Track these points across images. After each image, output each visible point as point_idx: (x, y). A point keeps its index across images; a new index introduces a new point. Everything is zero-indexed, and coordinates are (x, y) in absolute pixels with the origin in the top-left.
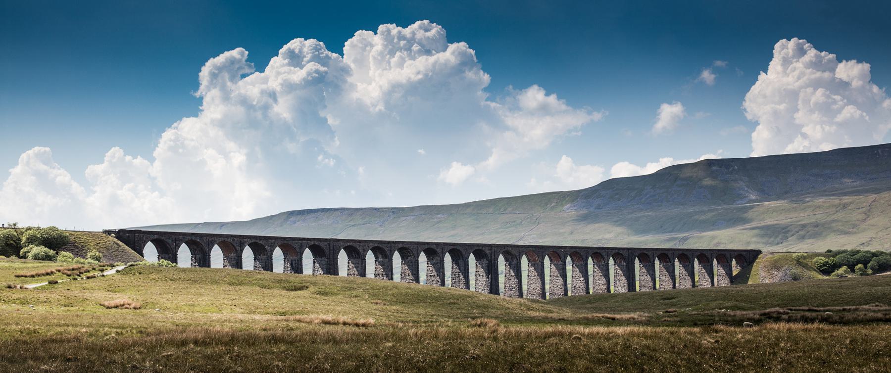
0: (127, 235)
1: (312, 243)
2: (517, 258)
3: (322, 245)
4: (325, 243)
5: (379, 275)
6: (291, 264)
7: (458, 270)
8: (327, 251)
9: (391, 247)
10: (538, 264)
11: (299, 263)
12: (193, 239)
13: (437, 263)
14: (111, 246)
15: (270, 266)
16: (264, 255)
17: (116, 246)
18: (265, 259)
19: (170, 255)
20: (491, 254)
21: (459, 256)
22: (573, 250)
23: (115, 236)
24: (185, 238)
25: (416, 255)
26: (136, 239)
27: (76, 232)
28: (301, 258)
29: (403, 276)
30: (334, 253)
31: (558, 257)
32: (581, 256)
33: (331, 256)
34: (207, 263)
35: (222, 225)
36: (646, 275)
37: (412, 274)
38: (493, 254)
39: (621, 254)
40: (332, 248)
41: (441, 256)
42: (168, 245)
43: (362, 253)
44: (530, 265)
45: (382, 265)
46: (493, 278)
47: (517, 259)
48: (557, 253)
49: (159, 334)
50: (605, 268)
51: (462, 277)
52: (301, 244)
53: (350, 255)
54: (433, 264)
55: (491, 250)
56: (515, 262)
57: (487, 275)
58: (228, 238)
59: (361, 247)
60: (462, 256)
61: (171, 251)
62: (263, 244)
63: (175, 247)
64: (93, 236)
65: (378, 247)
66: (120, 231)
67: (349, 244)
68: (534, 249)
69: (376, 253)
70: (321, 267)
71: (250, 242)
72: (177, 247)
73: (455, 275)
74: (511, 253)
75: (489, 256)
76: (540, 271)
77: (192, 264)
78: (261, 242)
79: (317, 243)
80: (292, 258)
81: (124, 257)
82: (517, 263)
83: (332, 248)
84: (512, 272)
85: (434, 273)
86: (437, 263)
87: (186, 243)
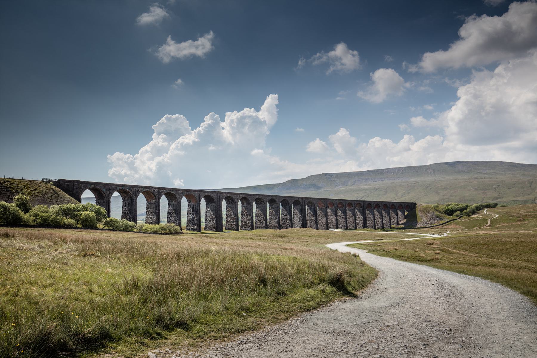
0: (67, 184)
1: (207, 194)
2: (314, 204)
3: (212, 195)
4: (215, 194)
5: (244, 214)
6: (193, 208)
7: (285, 212)
8: (215, 199)
9: (252, 197)
10: (324, 209)
11: (199, 207)
12: (124, 189)
13: (276, 207)
14: (48, 192)
15: (179, 208)
16: (175, 201)
17: (53, 192)
18: (176, 204)
19: (105, 200)
20: (303, 202)
21: (286, 203)
22: (340, 201)
23: (53, 184)
24: (117, 188)
25: (265, 203)
26: (75, 188)
27: (15, 179)
28: (200, 204)
29: (257, 215)
30: (220, 201)
31: (333, 205)
32: (343, 205)
33: (218, 202)
34: (134, 206)
35: (254, 188)
36: (370, 215)
37: (263, 214)
38: (304, 203)
39: (360, 204)
40: (218, 197)
41: (278, 203)
42: (103, 193)
43: (236, 201)
44: (319, 209)
45: (246, 208)
46: (304, 216)
47: (315, 206)
48: (332, 202)
49: (85, 255)
50: (353, 211)
51: (288, 216)
52: (200, 194)
53: (228, 202)
54: (273, 208)
55: (303, 200)
56: (313, 207)
57: (301, 214)
58: (150, 189)
59: (236, 197)
60: (288, 204)
61: (106, 198)
62: (175, 194)
63: (109, 194)
64: (32, 184)
65: (246, 197)
66: (60, 180)
67: (228, 195)
68: (322, 200)
69: (243, 201)
70: (211, 210)
71: (166, 192)
72: (110, 195)
73: (284, 214)
74: (311, 202)
75: (302, 204)
76: (325, 212)
77: (123, 207)
78: (173, 192)
79: (209, 194)
80: (193, 203)
81: (58, 201)
82: (315, 208)
83: (218, 197)
84: (311, 213)
85: (274, 213)
86: (276, 207)
87: (143, 193)
